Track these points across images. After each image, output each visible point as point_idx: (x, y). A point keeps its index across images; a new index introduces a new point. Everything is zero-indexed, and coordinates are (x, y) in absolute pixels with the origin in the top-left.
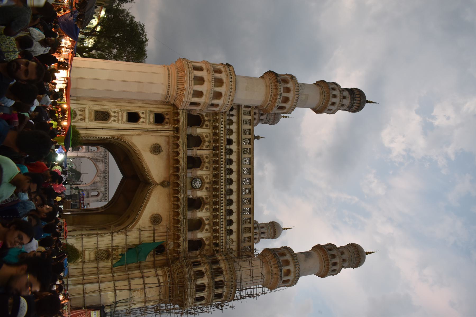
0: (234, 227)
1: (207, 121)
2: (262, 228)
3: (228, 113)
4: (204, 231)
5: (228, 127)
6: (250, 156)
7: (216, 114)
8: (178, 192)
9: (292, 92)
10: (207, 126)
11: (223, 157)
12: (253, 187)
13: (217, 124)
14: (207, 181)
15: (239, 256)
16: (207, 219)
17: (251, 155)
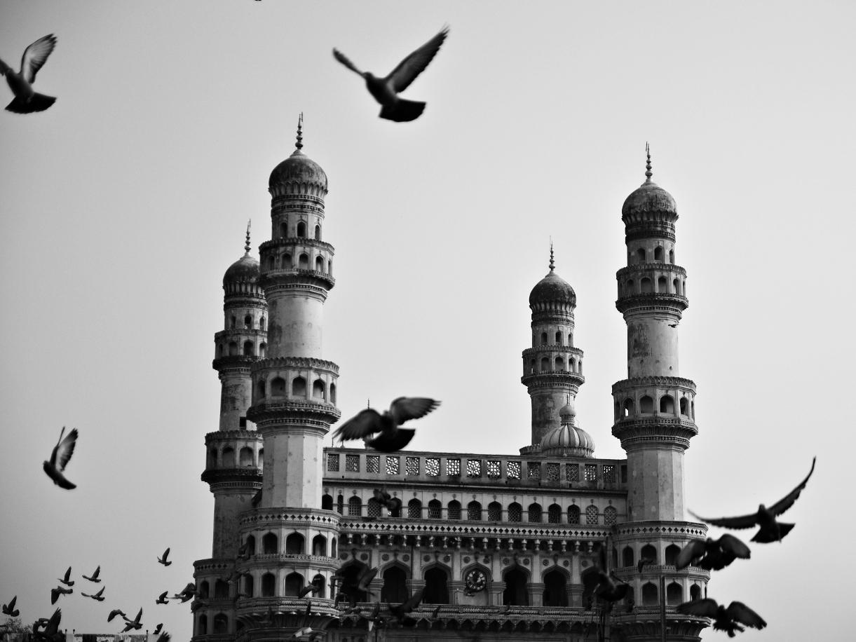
0: (565, 503)
1: (354, 557)
2: (545, 336)
3: (335, 509)
4: (568, 568)
5: (365, 512)
6: (423, 459)
7: (343, 538)
8: (495, 623)
9: (303, 374)
10: (364, 557)
11: (428, 527)
12: (486, 456)
13: (364, 536)
14: (472, 562)
15: (623, 495)
16: (546, 563)
17: (421, 458)
